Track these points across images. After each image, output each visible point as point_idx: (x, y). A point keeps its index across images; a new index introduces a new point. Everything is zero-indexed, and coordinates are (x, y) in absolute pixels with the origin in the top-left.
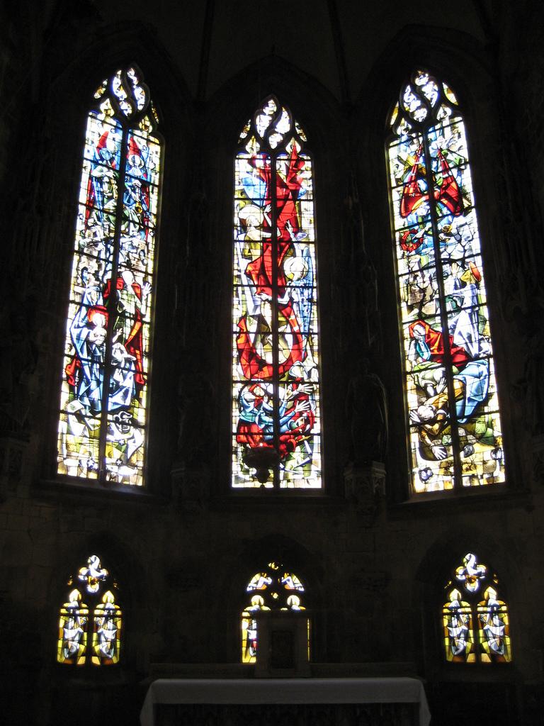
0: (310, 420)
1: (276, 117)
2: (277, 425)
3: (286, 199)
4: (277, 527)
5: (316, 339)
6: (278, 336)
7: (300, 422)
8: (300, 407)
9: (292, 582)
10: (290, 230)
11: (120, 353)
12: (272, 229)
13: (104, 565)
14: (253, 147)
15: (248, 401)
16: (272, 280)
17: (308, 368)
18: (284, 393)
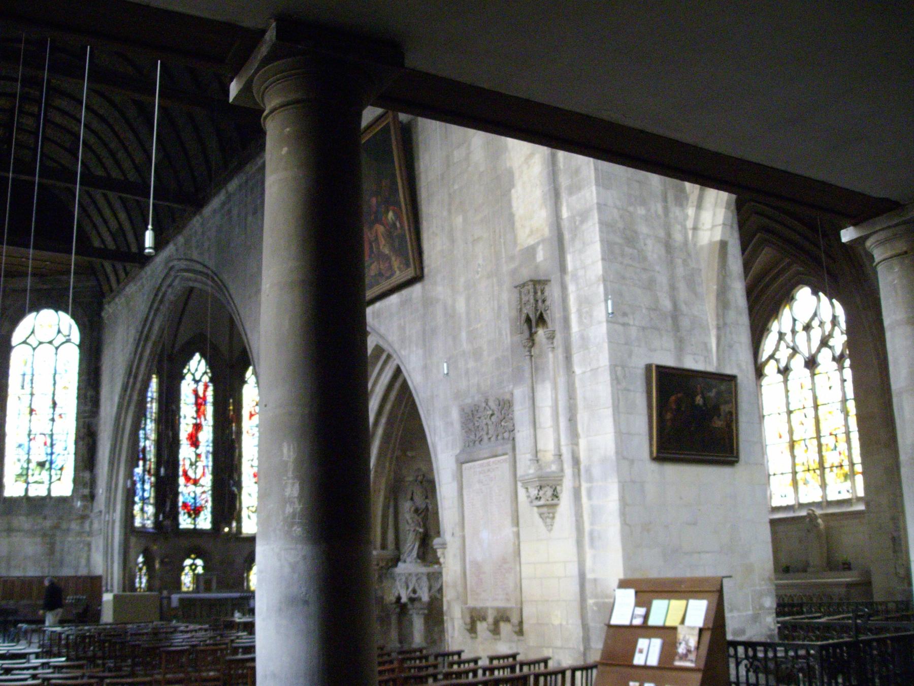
0: (207, 501)
1: (199, 362)
2: (195, 503)
3: (201, 404)
4: (195, 543)
5: (210, 468)
6: (196, 467)
7: (203, 502)
8: (204, 496)
9: (199, 562)
10: (203, 419)
11: (147, 477)
12: (196, 419)
13: (144, 557)
14: (189, 377)
15: (186, 492)
16: (195, 443)
17: (207, 481)
18: (199, 490)
